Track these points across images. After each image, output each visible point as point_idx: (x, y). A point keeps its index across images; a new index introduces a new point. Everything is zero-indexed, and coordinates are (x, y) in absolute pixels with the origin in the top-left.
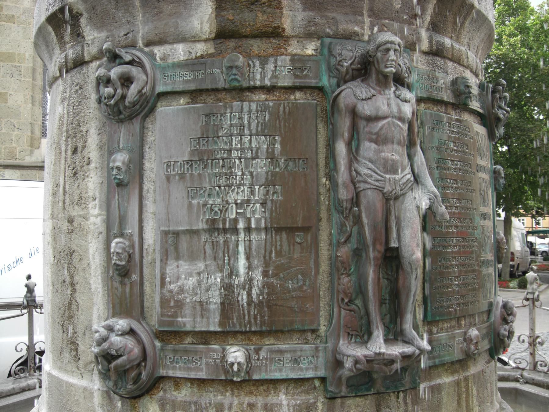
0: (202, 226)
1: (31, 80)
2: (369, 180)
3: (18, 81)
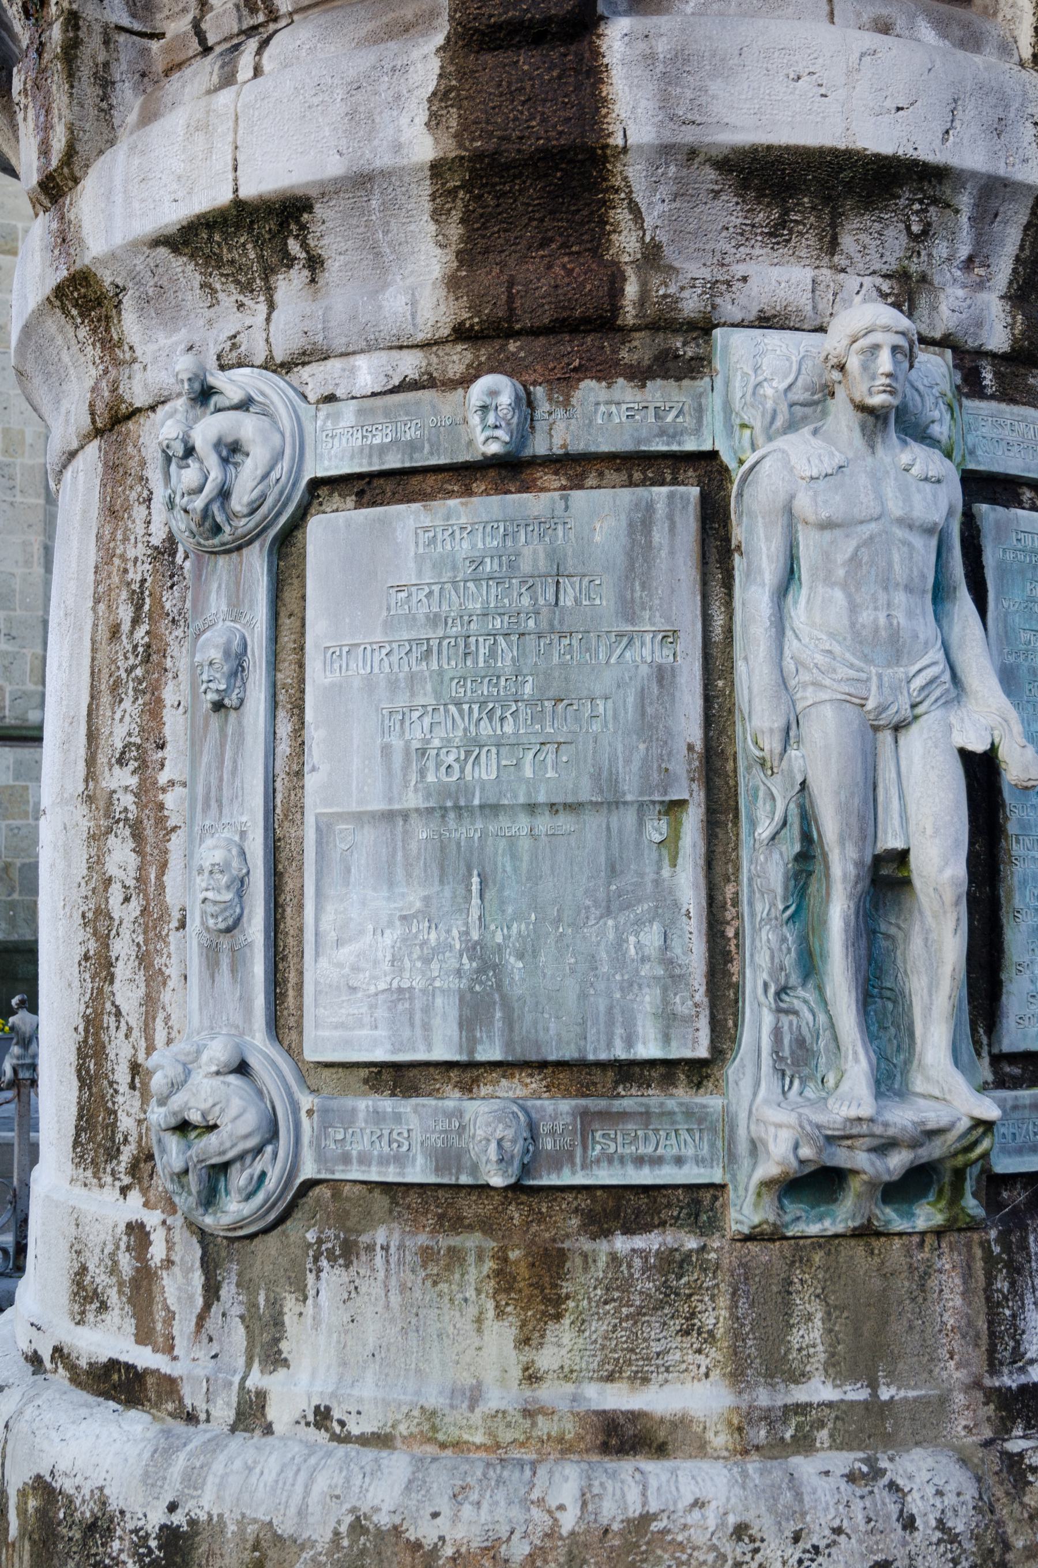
0: (413, 800)
1: (41, 501)
2: (827, 682)
3: (5, 506)
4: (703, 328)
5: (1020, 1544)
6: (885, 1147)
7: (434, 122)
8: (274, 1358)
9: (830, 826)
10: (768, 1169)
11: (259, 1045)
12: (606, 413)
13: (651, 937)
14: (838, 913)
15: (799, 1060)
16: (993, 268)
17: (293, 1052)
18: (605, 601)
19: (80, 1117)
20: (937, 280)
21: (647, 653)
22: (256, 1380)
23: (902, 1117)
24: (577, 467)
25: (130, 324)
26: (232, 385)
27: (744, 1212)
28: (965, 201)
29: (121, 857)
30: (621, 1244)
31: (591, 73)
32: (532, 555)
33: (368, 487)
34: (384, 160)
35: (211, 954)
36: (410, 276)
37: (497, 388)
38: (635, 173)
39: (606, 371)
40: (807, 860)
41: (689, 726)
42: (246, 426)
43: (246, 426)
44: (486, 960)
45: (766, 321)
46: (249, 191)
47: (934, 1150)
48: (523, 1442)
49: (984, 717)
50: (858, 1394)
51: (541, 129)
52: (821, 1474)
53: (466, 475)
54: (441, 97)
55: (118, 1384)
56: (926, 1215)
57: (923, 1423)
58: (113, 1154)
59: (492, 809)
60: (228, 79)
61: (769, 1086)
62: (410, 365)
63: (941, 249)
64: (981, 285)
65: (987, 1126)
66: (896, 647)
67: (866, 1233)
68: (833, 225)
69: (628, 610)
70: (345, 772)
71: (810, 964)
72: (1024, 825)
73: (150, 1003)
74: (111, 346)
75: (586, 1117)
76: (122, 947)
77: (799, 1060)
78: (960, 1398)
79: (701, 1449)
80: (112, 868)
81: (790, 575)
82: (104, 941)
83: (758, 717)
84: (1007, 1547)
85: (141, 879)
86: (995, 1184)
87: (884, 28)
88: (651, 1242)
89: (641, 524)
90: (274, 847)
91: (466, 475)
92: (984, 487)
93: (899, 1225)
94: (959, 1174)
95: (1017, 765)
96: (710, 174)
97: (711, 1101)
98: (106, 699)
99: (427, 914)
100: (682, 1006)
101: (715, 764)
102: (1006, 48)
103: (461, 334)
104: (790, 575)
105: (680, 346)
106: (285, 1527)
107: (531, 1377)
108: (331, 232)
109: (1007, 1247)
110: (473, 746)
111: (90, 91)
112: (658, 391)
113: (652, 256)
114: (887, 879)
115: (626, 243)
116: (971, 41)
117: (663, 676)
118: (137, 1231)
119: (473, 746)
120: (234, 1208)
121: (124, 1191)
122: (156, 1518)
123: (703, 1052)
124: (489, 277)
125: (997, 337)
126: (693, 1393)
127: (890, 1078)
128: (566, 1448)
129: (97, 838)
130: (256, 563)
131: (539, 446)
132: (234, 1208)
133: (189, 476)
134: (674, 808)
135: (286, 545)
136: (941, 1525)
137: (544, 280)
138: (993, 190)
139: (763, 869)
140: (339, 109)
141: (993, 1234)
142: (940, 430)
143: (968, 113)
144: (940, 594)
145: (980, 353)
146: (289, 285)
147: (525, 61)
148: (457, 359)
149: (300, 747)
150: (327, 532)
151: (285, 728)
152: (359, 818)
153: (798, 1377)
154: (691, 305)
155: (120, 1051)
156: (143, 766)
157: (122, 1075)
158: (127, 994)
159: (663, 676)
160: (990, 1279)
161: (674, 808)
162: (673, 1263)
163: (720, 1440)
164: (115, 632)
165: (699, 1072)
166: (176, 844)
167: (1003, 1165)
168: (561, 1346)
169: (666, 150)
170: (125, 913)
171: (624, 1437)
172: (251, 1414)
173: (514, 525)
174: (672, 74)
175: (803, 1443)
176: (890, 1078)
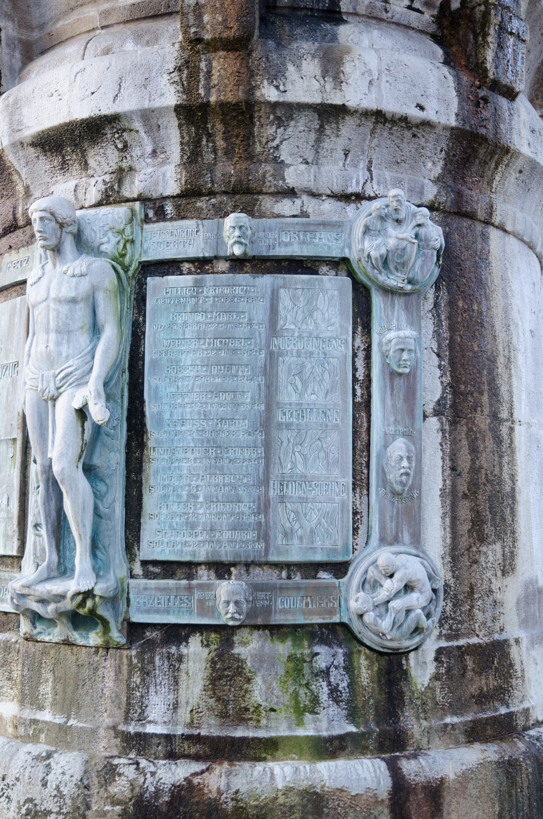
5: (94, 808)
16: (168, 153)
20: (137, 167)
23: (55, 587)
28: (137, 125)
56: (94, 638)
63: (136, 152)
64: (164, 163)
68: (84, 156)
72: (159, 442)
78: (102, 732)
84: (88, 807)
93: (80, 641)
96: (31, 150)
109: (142, 661)
123: (14, 553)
125: (172, 188)
136: (58, 788)
138: (148, 116)
141: (134, 653)
145: (165, 198)
153: (41, 708)
160: (130, 674)
167: (137, 618)
176: (63, 569)
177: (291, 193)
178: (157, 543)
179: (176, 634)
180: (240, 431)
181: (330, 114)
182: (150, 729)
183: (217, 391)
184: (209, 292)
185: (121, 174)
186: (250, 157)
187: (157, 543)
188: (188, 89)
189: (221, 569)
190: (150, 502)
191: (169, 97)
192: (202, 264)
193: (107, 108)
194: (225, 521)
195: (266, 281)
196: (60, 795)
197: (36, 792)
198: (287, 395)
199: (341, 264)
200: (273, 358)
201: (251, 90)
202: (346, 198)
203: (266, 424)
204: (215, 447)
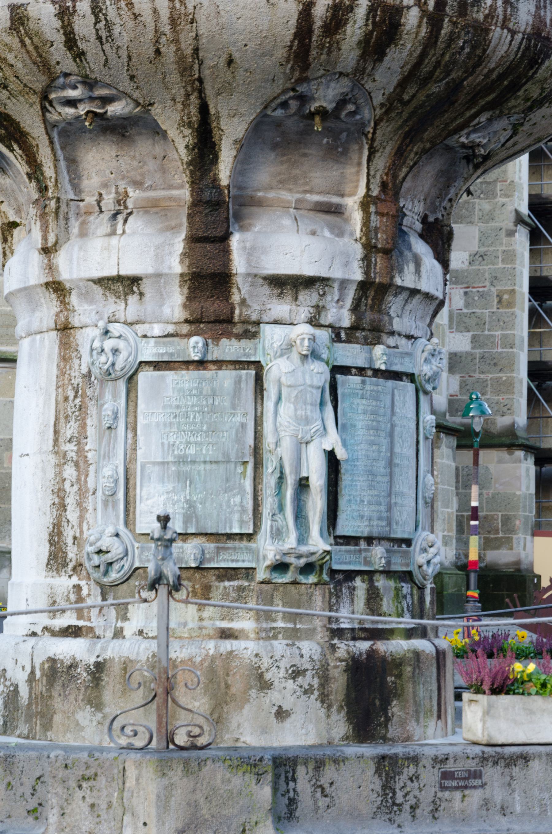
0: (170, 459)
4: (258, 323)
5: (332, 664)
6: (299, 557)
7: (182, 262)
8: (125, 618)
9: (287, 470)
10: (268, 563)
11: (122, 529)
12: (230, 348)
13: (238, 499)
14: (289, 493)
15: (278, 534)
17: (132, 531)
18: (227, 404)
19: (50, 555)
20: (328, 307)
21: (239, 419)
22: (119, 624)
23: (304, 549)
24: (219, 364)
25: (74, 299)
26: (116, 329)
27: (261, 575)
28: (336, 285)
29: (70, 472)
30: (227, 584)
31: (227, 252)
32: (207, 389)
33: (157, 365)
34: (166, 271)
35: (105, 504)
36: (174, 304)
37: (197, 341)
38: (239, 280)
39: (229, 335)
40: (281, 478)
41: (250, 441)
42: (121, 344)
43: (121, 344)
44: (191, 504)
45: (276, 322)
46: (123, 273)
47: (313, 559)
48: (200, 634)
49: (332, 440)
50: (290, 625)
51: (212, 267)
52: (279, 646)
53: (188, 364)
54: (184, 254)
55: (73, 632)
56: (312, 579)
57: (309, 634)
58: (65, 565)
59: (193, 462)
60: (113, 233)
61: (269, 540)
62: (171, 329)
63: (329, 298)
64: (342, 307)
65: (328, 552)
66: (307, 421)
67: (295, 583)
68: (296, 293)
69: (234, 407)
70: (149, 450)
71: (281, 508)
72: (346, 470)
73: (81, 518)
74: (64, 303)
75: (218, 548)
76: (70, 501)
77: (278, 534)
78: (319, 629)
79: (247, 638)
80: (66, 475)
81: (279, 399)
82: (63, 499)
83: (269, 439)
84: (328, 665)
85: (78, 480)
86: (333, 572)
87: (313, 233)
88: (235, 583)
89: (238, 381)
90: (126, 471)
91: (188, 364)
92: (338, 370)
93: (304, 581)
94: (321, 567)
95: (340, 454)
96: (261, 280)
97: (253, 545)
98: (62, 421)
99: (174, 491)
100: (245, 518)
101: (257, 451)
102: (352, 234)
103: (187, 321)
104: (279, 399)
105: (250, 331)
106: (133, 657)
107: (201, 619)
108: (146, 286)
109: (336, 590)
110: (188, 443)
111: (62, 222)
112: (244, 343)
113: (243, 302)
114: (303, 485)
115: (236, 298)
116: (341, 234)
117: (243, 426)
118: (78, 588)
119: (188, 443)
120: (114, 575)
121: (70, 576)
122: (92, 660)
123: (251, 531)
124: (196, 305)
125: (346, 323)
126: (245, 623)
127: (302, 539)
128: (210, 638)
129: (60, 466)
130: (122, 386)
131: (209, 357)
132: (114, 575)
133: (103, 359)
134: (245, 463)
135: (131, 380)
136: (310, 657)
137: (212, 307)
139: (269, 481)
140: (152, 253)
141: (332, 586)
142: (325, 356)
143: (337, 261)
144: (322, 404)
145: (340, 328)
146: (133, 299)
147: (209, 247)
148: (186, 328)
149: (135, 442)
150: (145, 377)
151: (130, 435)
152: (154, 463)
153: (274, 621)
154: (254, 317)
155: (68, 534)
156: (79, 443)
157: (70, 541)
158: (72, 514)
159: (243, 426)
160: (330, 598)
161: (245, 463)
162: (241, 589)
163: (252, 636)
164: (66, 399)
165: (250, 537)
166: (92, 469)
167: (335, 567)
168: (208, 612)
169: (248, 275)
170: (71, 491)
171: (226, 634)
172: (118, 634)
173: (202, 380)
174: (250, 253)
175: (275, 637)
176: (302, 539)
177: (392, 333)
178: (345, 527)
179: (350, 575)
180: (381, 467)
181: (414, 292)
182: (343, 626)
183: (372, 443)
184: (368, 387)
185: (319, 309)
186: (380, 311)
187: (345, 527)
188: (367, 273)
189: (370, 540)
190: (342, 503)
191: (358, 276)
192: (361, 371)
193: (324, 274)
194: (375, 515)
195: (390, 383)
196: (312, 660)
197: (297, 661)
198: (397, 450)
199: (411, 377)
200: (393, 426)
201: (392, 278)
202: (409, 337)
203: (391, 464)
204: (371, 473)
